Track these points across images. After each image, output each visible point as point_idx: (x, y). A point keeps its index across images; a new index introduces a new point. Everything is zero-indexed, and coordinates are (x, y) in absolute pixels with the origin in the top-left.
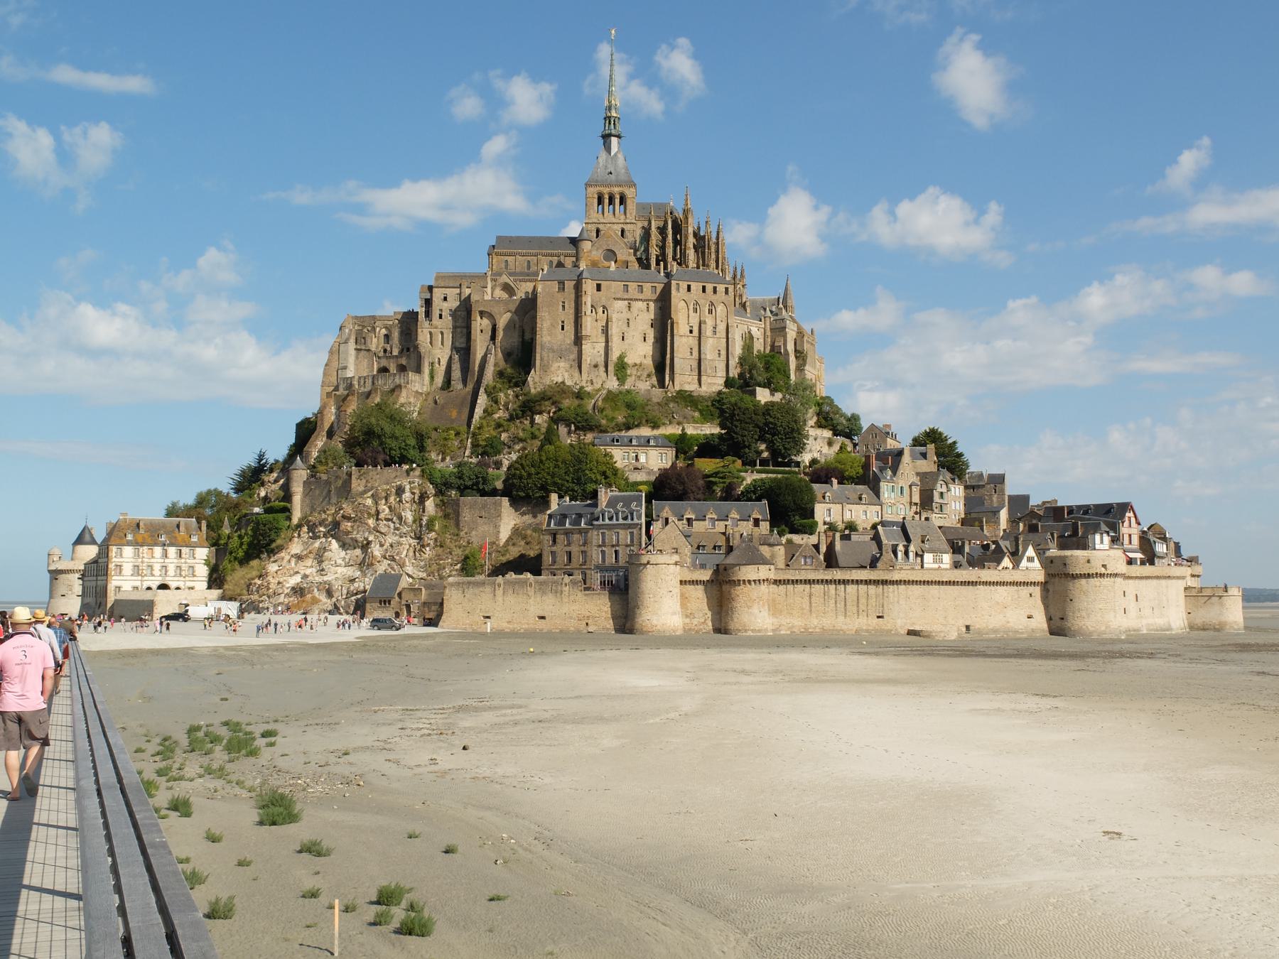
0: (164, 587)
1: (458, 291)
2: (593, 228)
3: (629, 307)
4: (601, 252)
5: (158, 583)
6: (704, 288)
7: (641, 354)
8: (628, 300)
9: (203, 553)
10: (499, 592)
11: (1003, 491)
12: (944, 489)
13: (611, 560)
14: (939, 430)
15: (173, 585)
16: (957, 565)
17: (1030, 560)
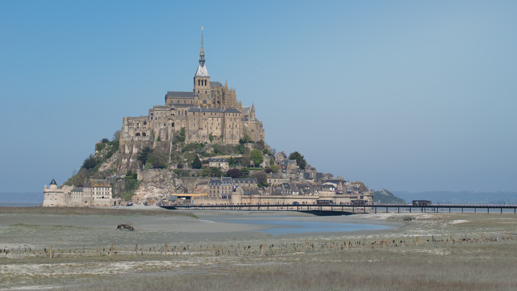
0: (103, 197)
1: (162, 111)
2: (198, 90)
3: (213, 119)
4: (202, 101)
5: (102, 197)
6: (233, 114)
7: (216, 133)
8: (212, 117)
9: (111, 189)
10: (203, 200)
11: (314, 172)
12: (298, 174)
13: (224, 193)
14: (298, 153)
15: (105, 197)
16: (300, 194)
17: (316, 193)
